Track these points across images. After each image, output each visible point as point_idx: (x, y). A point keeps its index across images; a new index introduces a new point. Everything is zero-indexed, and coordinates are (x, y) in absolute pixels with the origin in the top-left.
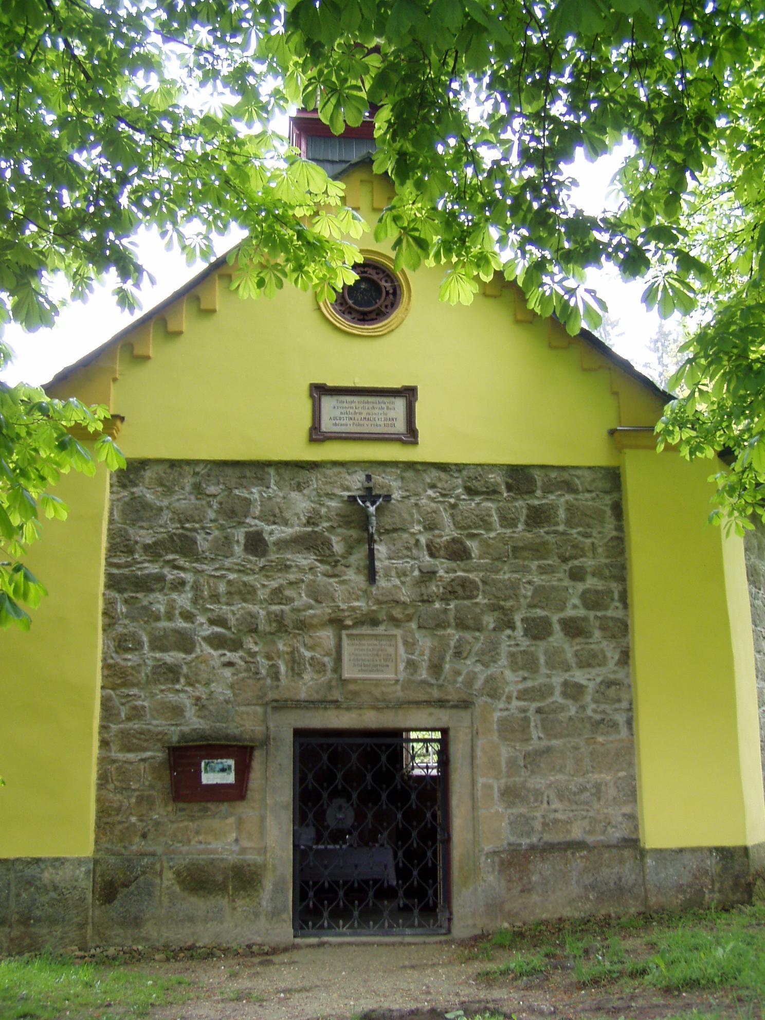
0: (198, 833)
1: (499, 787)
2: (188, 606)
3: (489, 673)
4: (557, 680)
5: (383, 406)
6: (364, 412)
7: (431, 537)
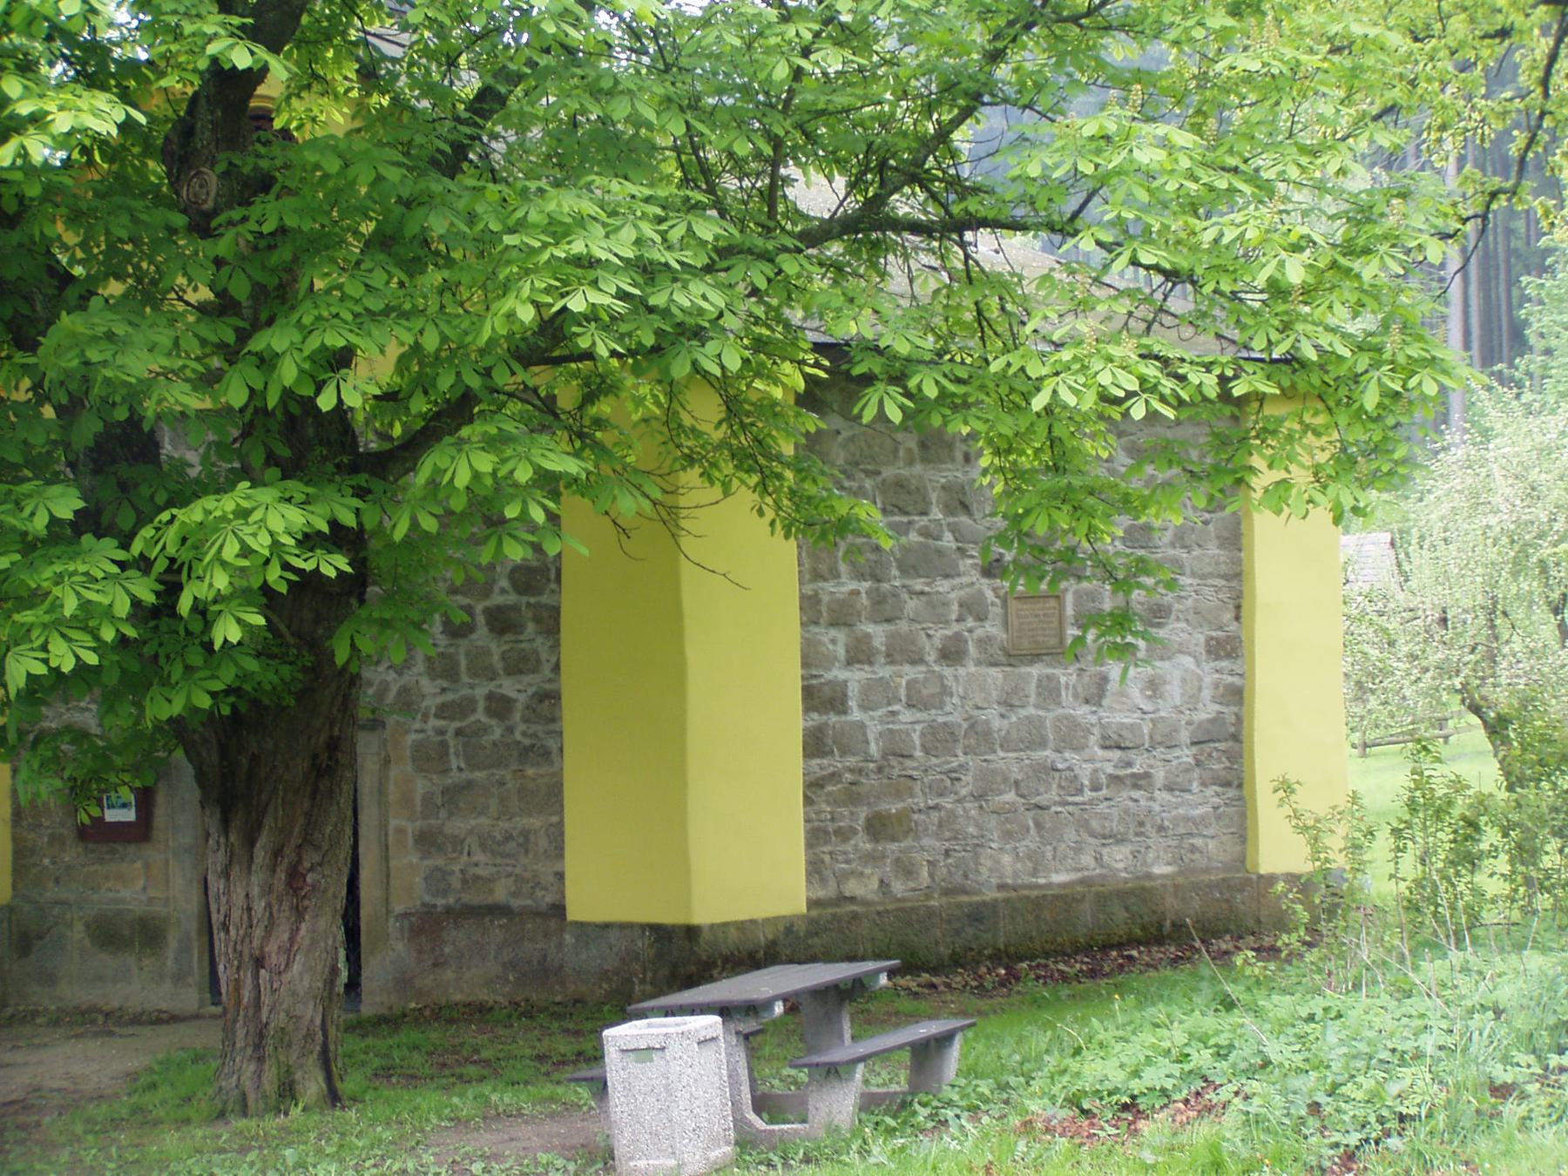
0: (107, 878)
4: (480, 692)
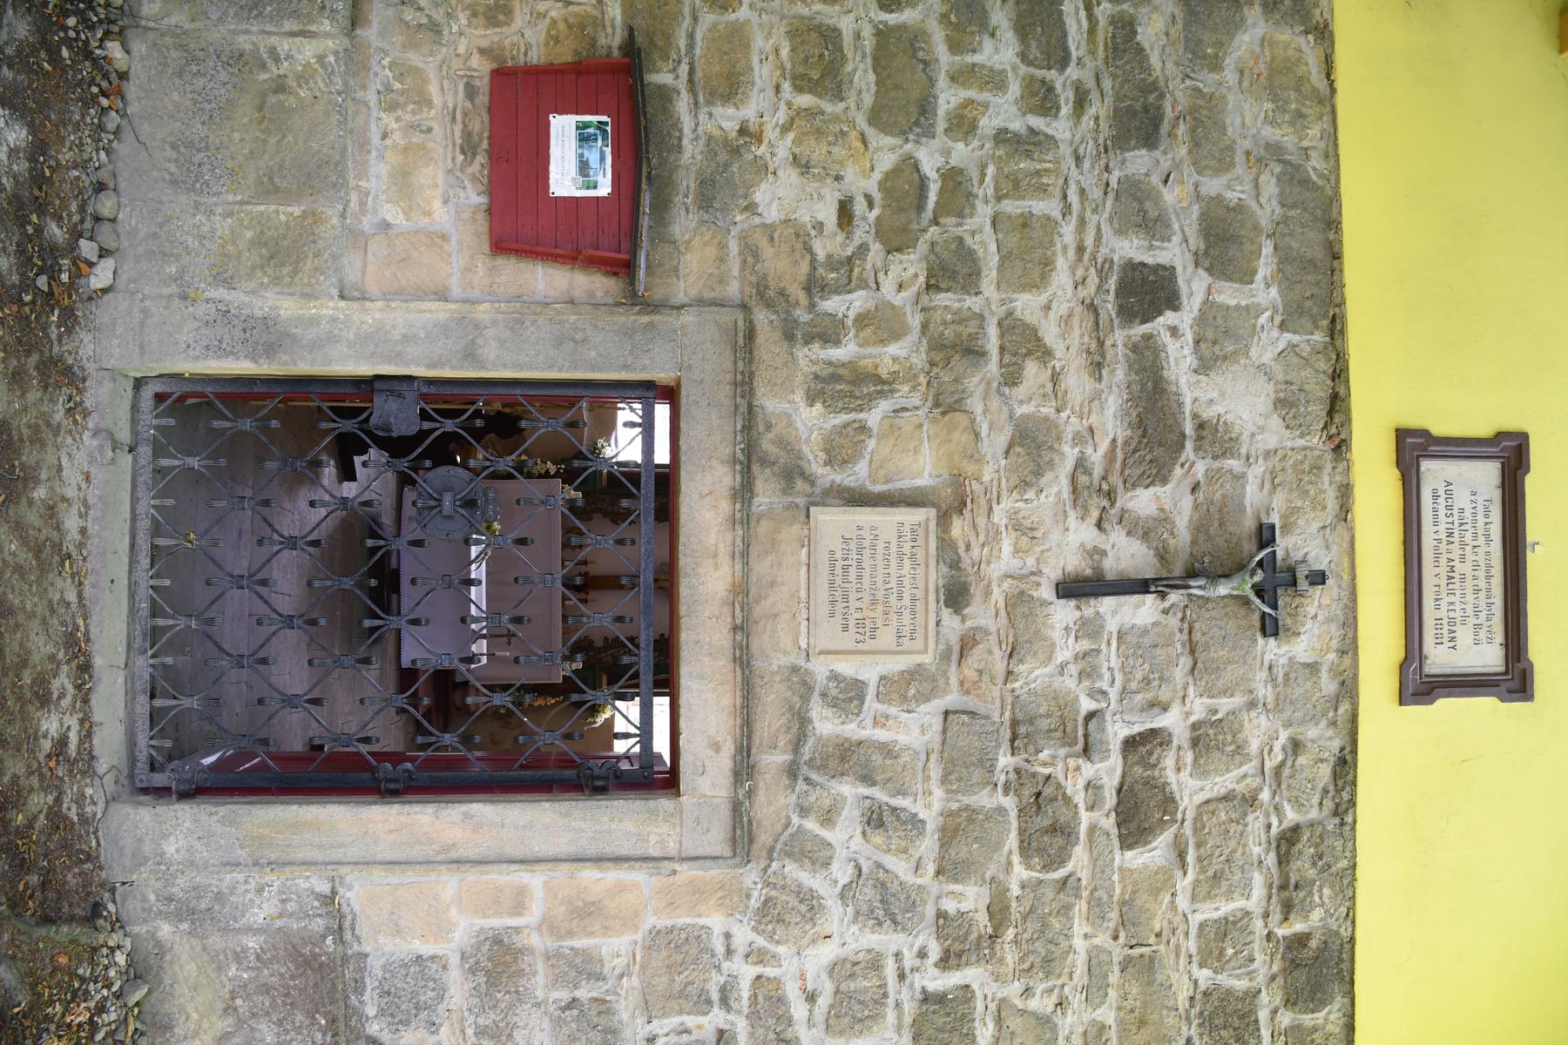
1: (517, 930)
2: (988, 124)
3: (828, 903)
5: (1483, 615)
6: (1467, 568)
7: (1175, 742)
